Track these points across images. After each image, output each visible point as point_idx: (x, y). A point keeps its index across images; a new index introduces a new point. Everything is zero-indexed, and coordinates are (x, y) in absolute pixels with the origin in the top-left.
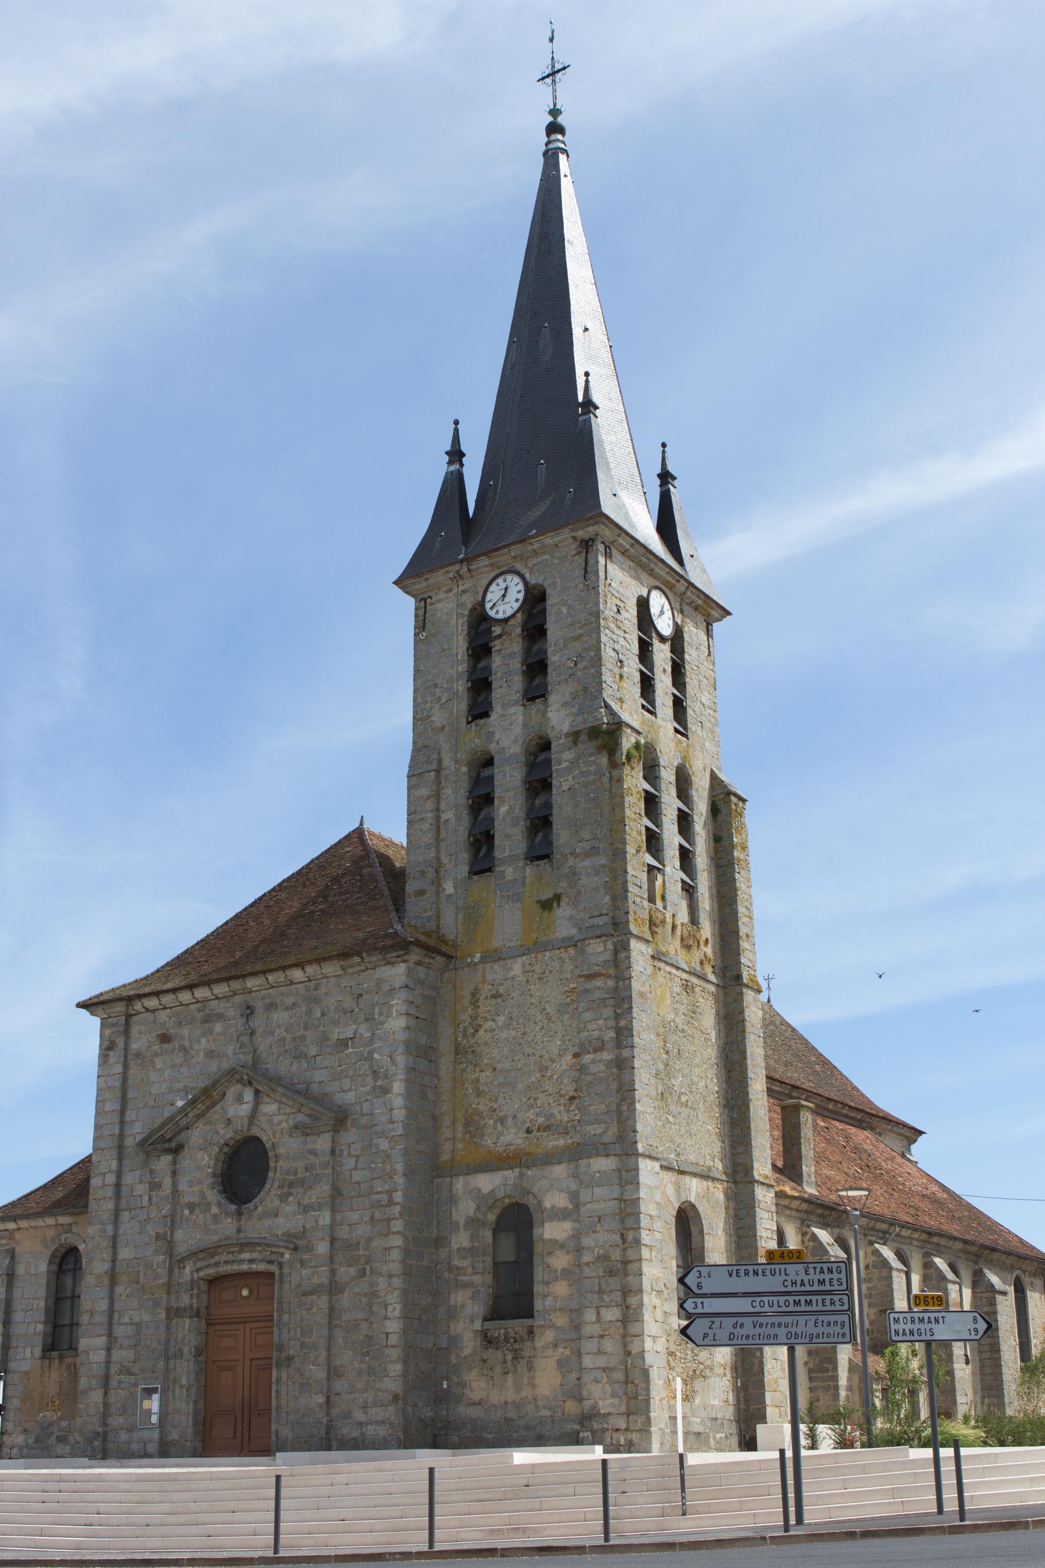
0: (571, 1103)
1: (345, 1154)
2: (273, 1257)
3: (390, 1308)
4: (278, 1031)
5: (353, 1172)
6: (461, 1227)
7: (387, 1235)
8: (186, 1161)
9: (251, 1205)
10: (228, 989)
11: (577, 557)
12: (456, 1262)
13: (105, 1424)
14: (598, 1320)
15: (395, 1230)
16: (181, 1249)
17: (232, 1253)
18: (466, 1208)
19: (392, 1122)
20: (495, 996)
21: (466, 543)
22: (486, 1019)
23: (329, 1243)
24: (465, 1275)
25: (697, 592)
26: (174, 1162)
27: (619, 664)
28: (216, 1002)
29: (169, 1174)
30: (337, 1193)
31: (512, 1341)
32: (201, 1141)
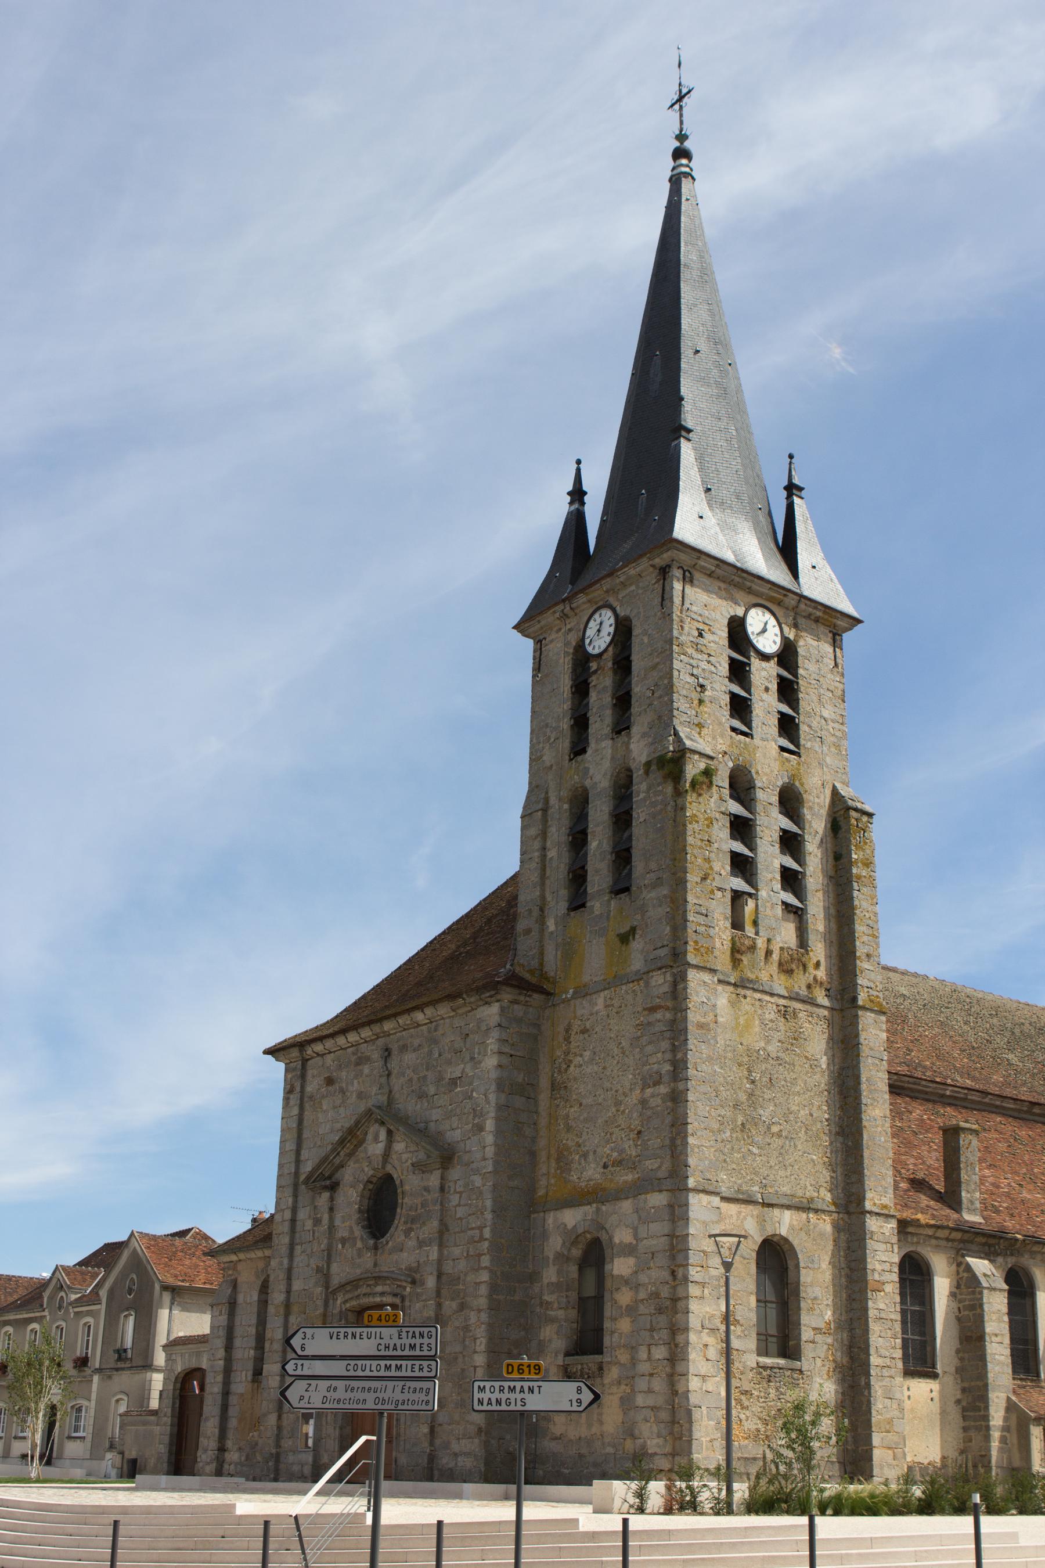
0: (638, 1138)
1: (452, 1190)
2: (398, 1291)
3: (478, 1342)
4: (408, 1072)
5: (457, 1208)
6: (551, 1261)
7: (477, 1270)
8: (340, 1199)
9: (383, 1240)
10: (371, 1033)
11: (656, 586)
12: (546, 1298)
13: (278, 1445)
14: (649, 1359)
15: (484, 1265)
16: (335, 1281)
17: (368, 1285)
18: (555, 1244)
19: (485, 1159)
20: (584, 1031)
21: (573, 582)
22: (576, 1055)
23: (435, 1277)
24: (552, 1309)
26: (332, 1199)
27: (699, 689)
28: (365, 1045)
29: (327, 1210)
30: (444, 1229)
31: (586, 1376)
32: (351, 1179)
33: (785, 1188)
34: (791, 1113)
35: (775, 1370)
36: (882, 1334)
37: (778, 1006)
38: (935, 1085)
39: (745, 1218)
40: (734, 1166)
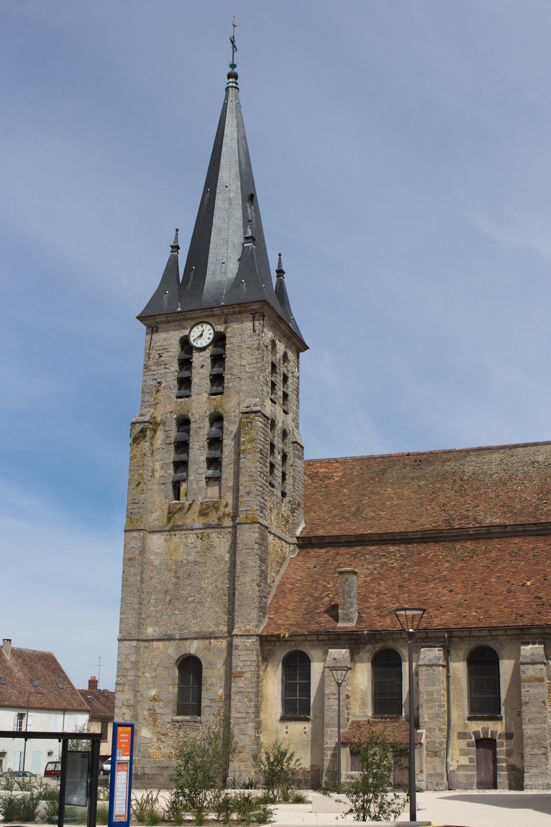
25: (231, 307)
34: (202, 589)
35: (184, 723)
37: (196, 534)
39: (168, 648)
40: (163, 623)
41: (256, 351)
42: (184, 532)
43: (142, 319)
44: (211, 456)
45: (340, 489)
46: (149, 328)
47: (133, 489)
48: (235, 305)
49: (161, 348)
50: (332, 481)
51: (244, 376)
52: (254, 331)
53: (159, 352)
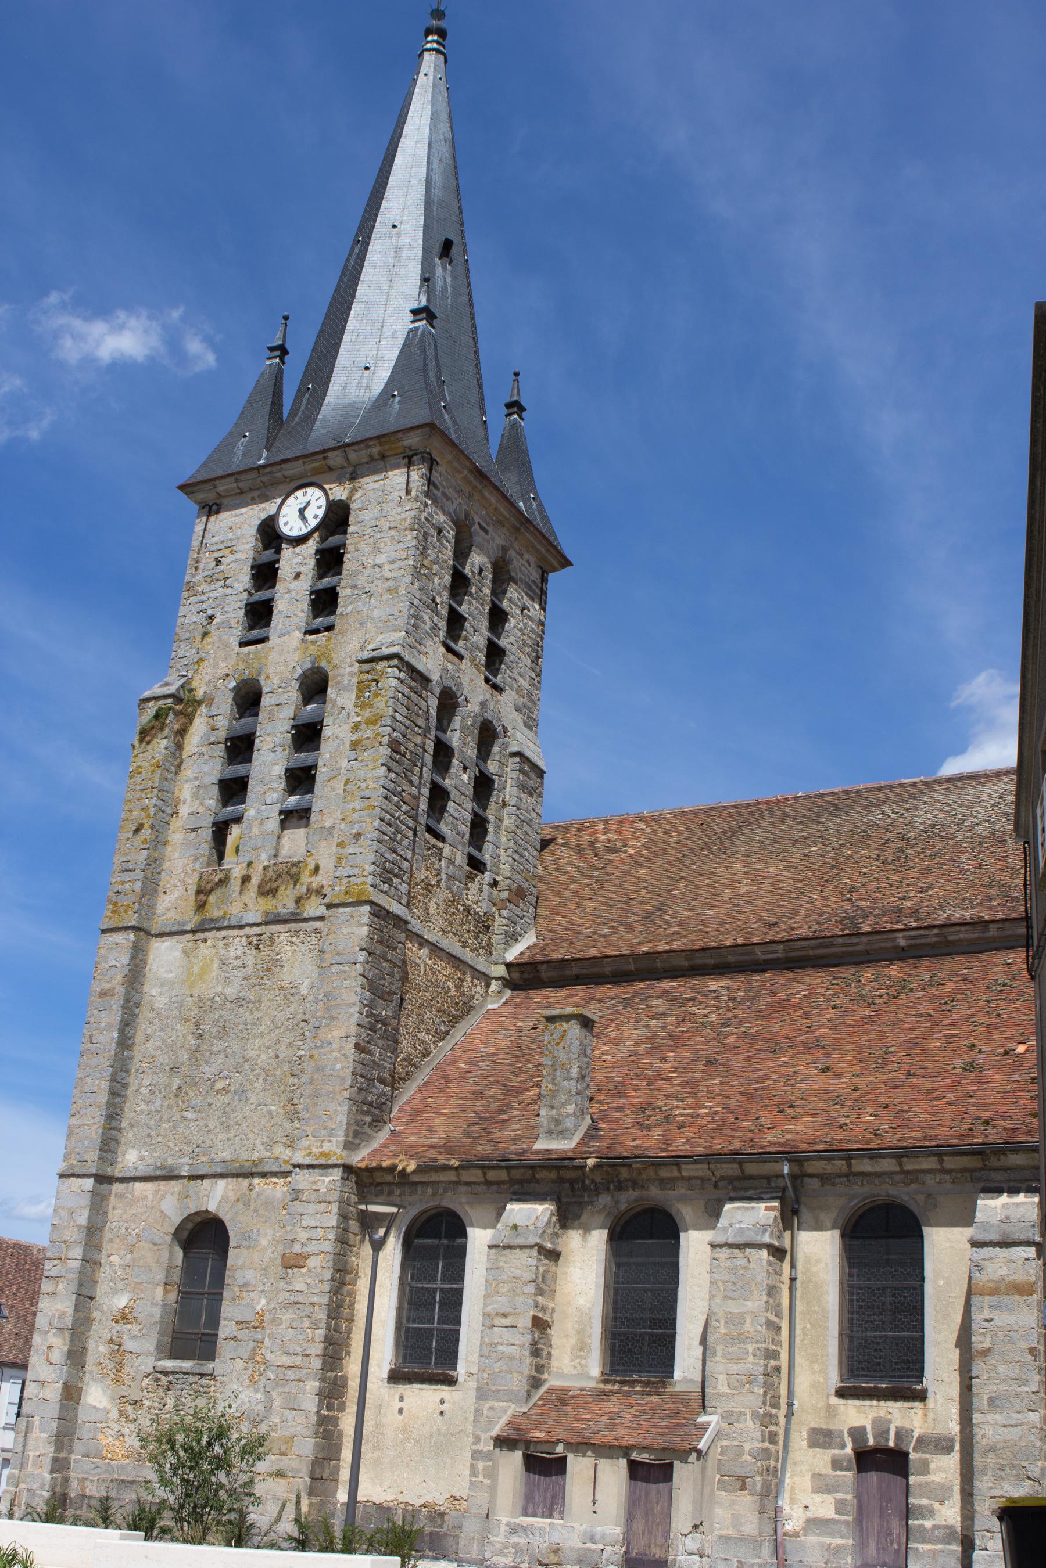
33: (224, 1154)
34: (247, 1061)
35: (177, 1376)
36: (294, 1325)
37: (248, 937)
38: (864, 939)
39: (163, 1197)
40: (160, 1139)
41: (407, 532)
42: (223, 933)
43: (190, 489)
44: (294, 764)
45: (634, 870)
46: (204, 508)
47: (128, 839)
48: (371, 439)
49: (222, 546)
50: (619, 856)
51: (379, 587)
52: (408, 492)
53: (216, 555)
